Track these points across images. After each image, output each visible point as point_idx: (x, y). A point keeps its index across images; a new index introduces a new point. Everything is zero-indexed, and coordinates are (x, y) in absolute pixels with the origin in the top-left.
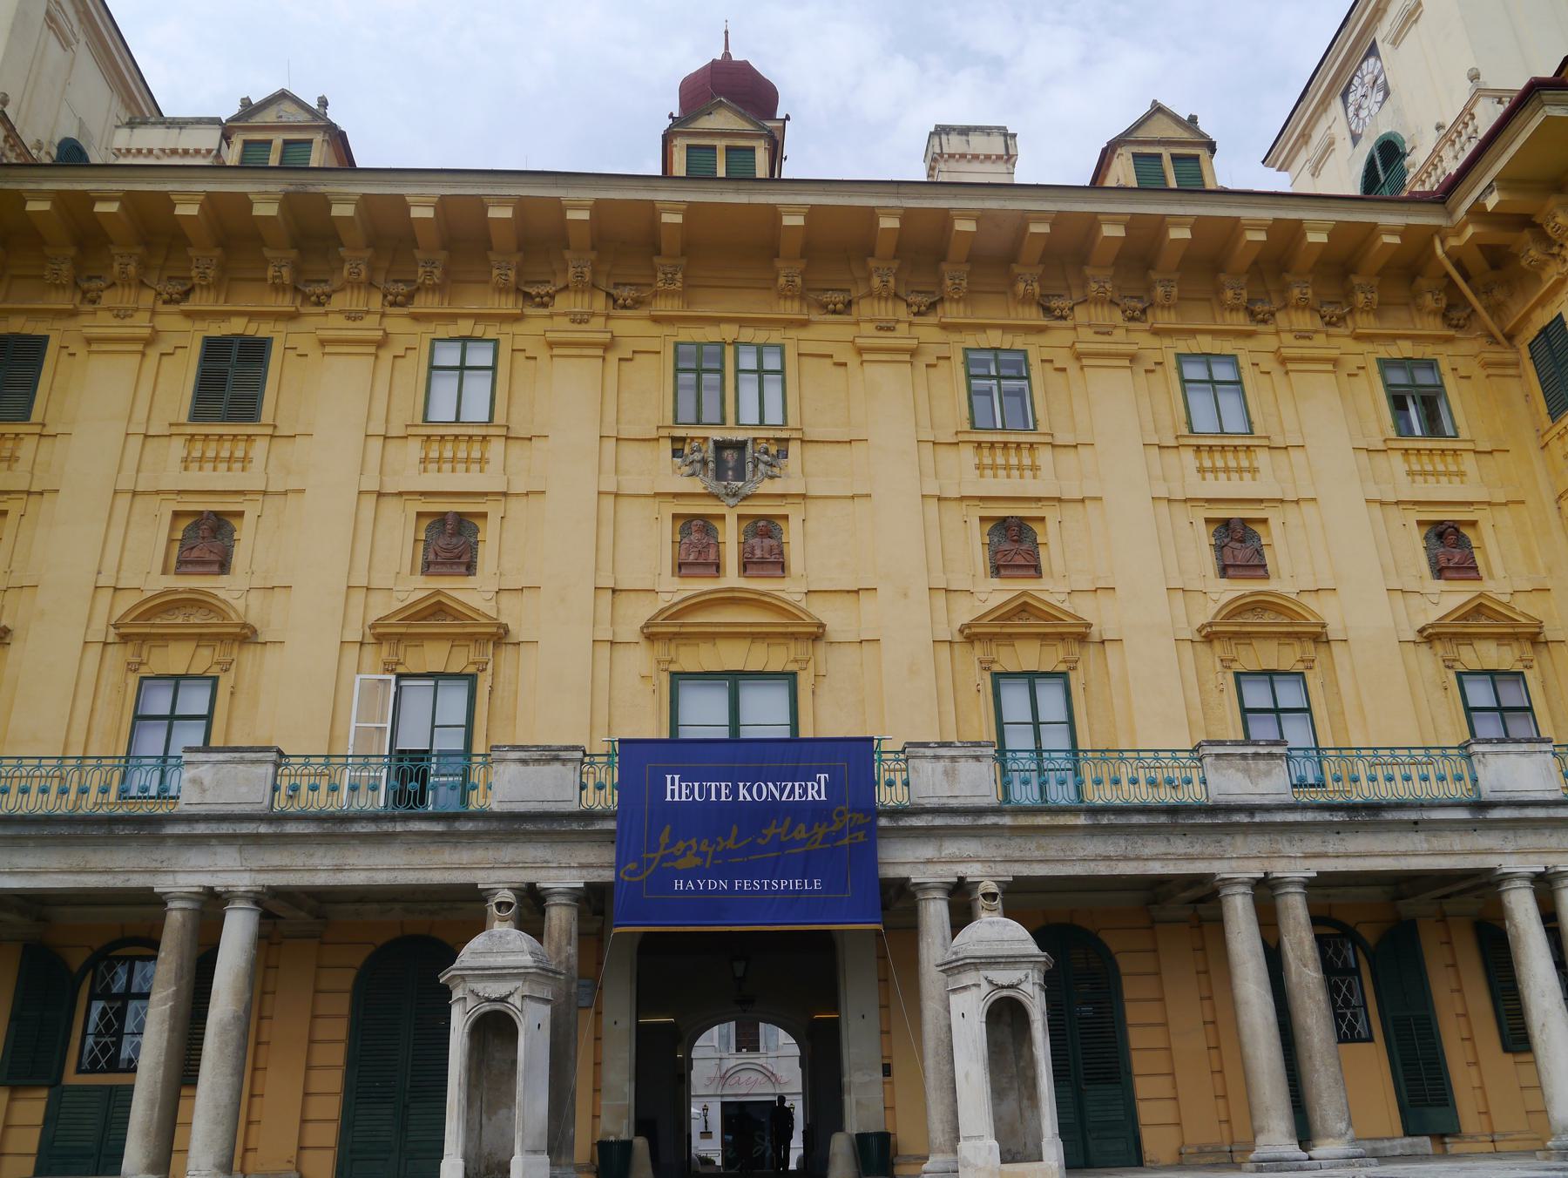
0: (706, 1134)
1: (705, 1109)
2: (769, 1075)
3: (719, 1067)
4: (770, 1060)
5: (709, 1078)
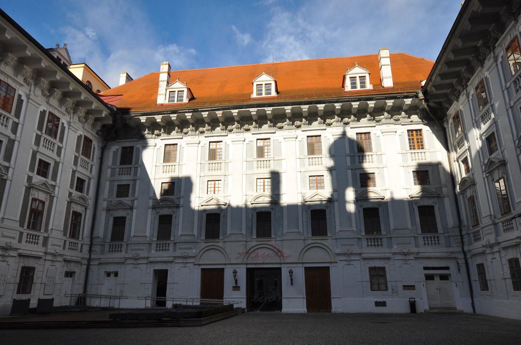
0: (236, 288)
1: (235, 272)
2: (277, 251)
3: (245, 246)
4: (277, 242)
5: (239, 253)
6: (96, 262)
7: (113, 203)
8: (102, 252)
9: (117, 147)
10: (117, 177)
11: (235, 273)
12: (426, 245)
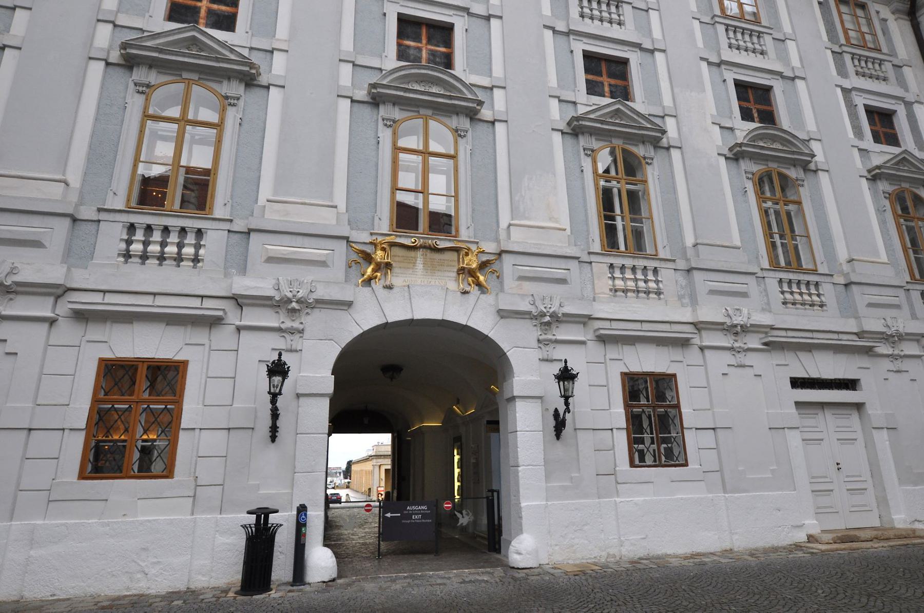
11: (277, 379)
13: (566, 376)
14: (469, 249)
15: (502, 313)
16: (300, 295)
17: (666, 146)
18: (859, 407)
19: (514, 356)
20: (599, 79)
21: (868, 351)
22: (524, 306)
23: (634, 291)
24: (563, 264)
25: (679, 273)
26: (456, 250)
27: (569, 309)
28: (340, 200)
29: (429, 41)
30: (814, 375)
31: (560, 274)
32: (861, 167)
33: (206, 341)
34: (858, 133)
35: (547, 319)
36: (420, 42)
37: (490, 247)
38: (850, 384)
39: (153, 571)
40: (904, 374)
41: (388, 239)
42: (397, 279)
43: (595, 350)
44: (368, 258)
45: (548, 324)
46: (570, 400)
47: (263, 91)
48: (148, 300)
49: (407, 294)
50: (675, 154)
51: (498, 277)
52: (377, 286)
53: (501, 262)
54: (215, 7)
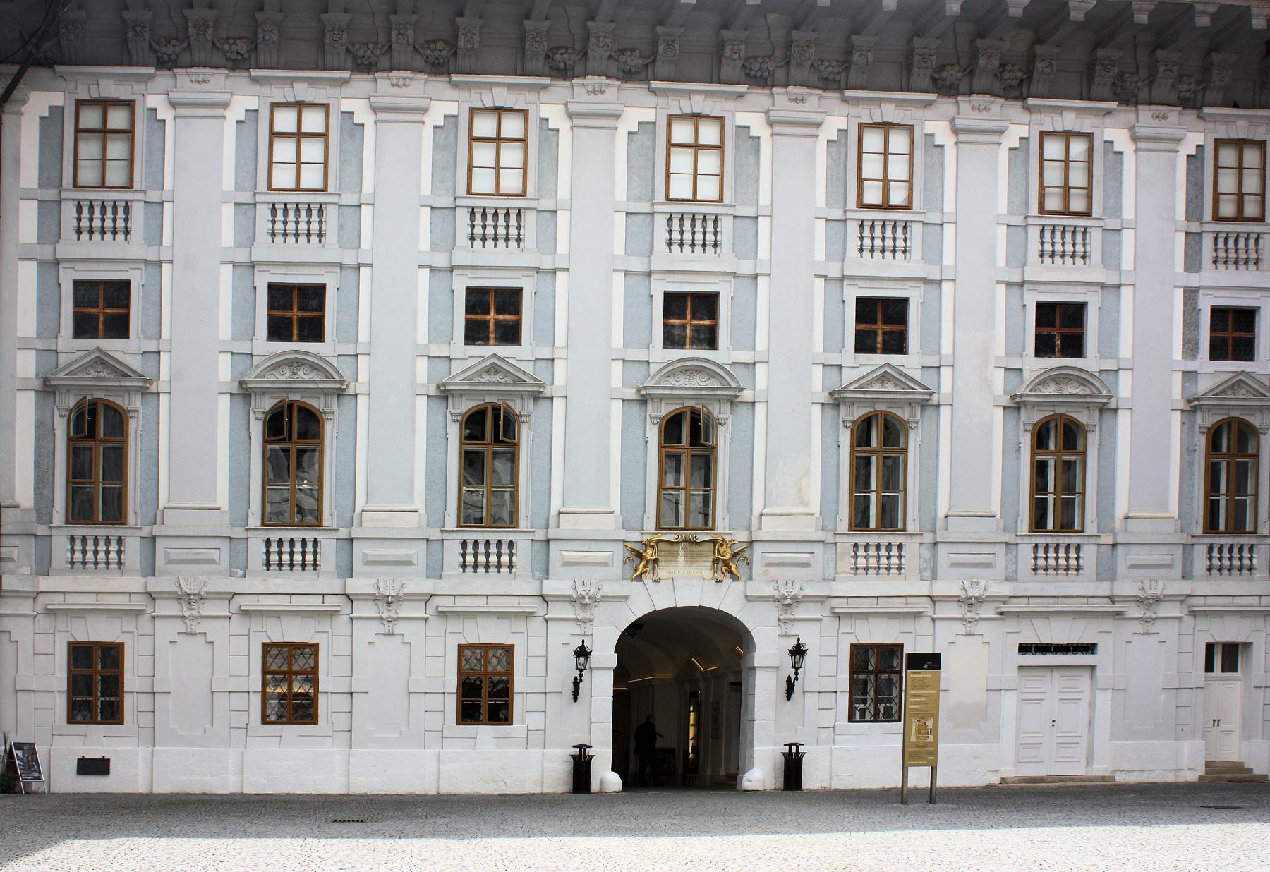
6: (26, 607)
7: (63, 359)
8: (44, 567)
9: (57, 99)
10: (69, 247)
11: (582, 659)
12: (1215, 572)
13: (798, 651)
14: (724, 540)
15: (750, 598)
16: (591, 593)
17: (936, 404)
18: (1093, 668)
19: (756, 633)
20: (874, 327)
21: (1118, 615)
22: (769, 590)
23: (875, 568)
24: (808, 548)
25: (924, 547)
26: (714, 542)
27: (809, 591)
28: (615, 504)
29: (693, 318)
30: (1045, 641)
31: (804, 557)
32: (1179, 397)
33: (524, 629)
34: (1190, 348)
35: (789, 601)
36: (685, 318)
37: (742, 536)
38: (1088, 648)
39: (508, 781)
40: (1155, 636)
41: (657, 537)
42: (662, 572)
43: (830, 625)
44: (640, 556)
45: (789, 605)
46: (800, 671)
47: (548, 403)
48: (482, 601)
49: (671, 586)
50: (945, 412)
51: (748, 564)
52: (648, 582)
53: (751, 549)
54: (501, 317)
